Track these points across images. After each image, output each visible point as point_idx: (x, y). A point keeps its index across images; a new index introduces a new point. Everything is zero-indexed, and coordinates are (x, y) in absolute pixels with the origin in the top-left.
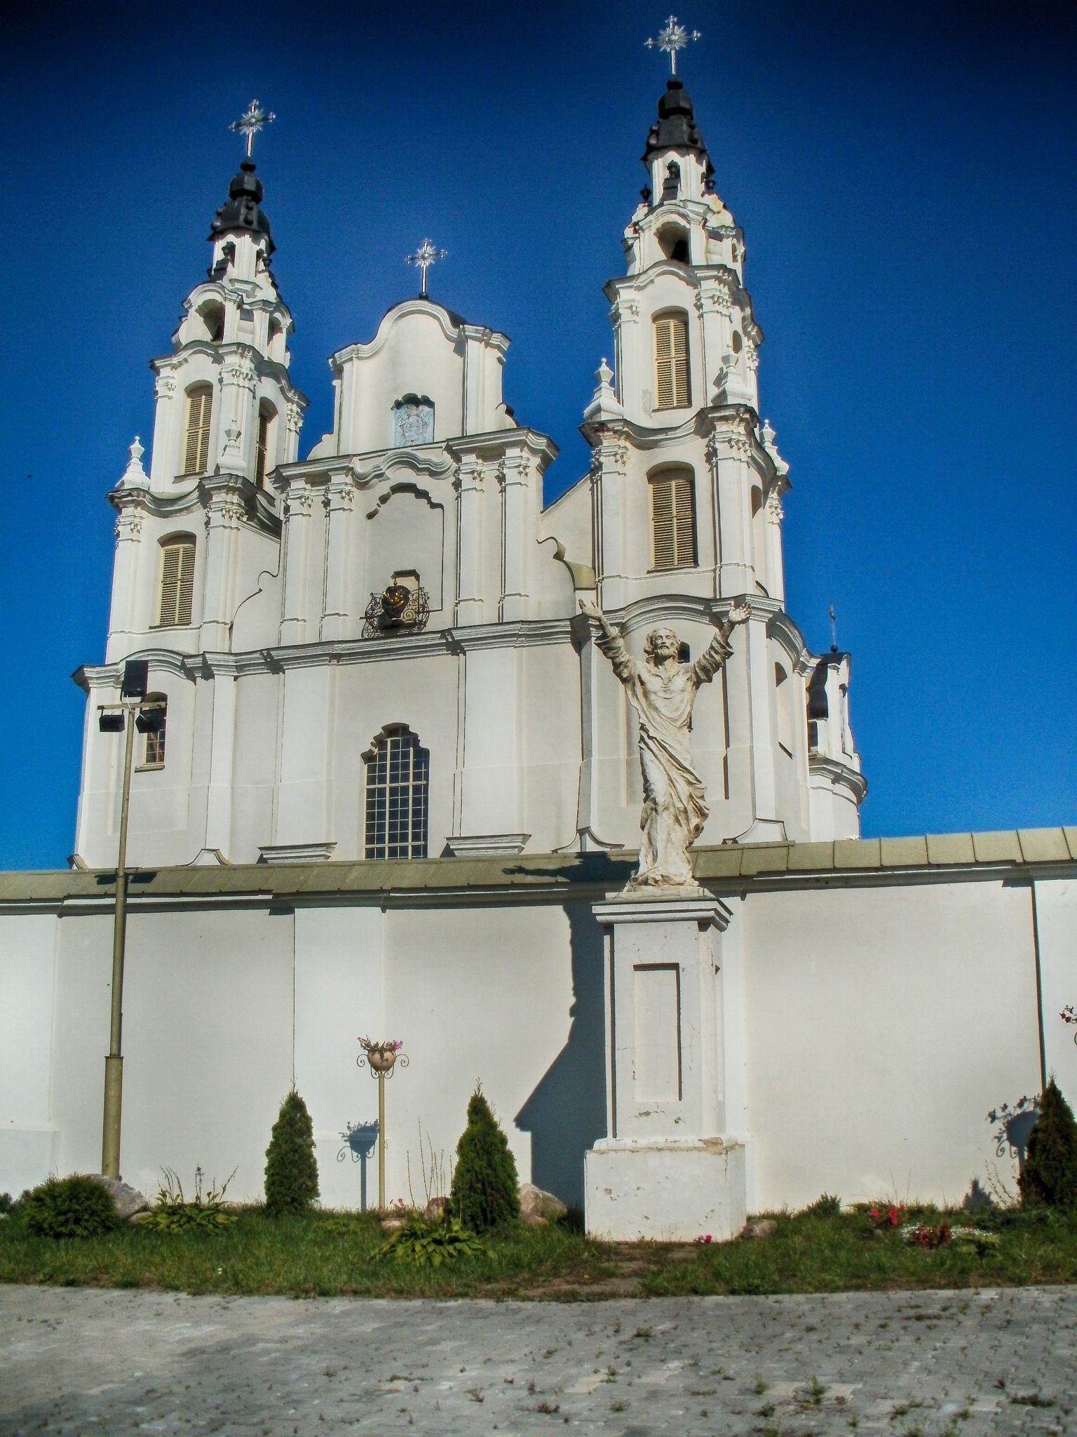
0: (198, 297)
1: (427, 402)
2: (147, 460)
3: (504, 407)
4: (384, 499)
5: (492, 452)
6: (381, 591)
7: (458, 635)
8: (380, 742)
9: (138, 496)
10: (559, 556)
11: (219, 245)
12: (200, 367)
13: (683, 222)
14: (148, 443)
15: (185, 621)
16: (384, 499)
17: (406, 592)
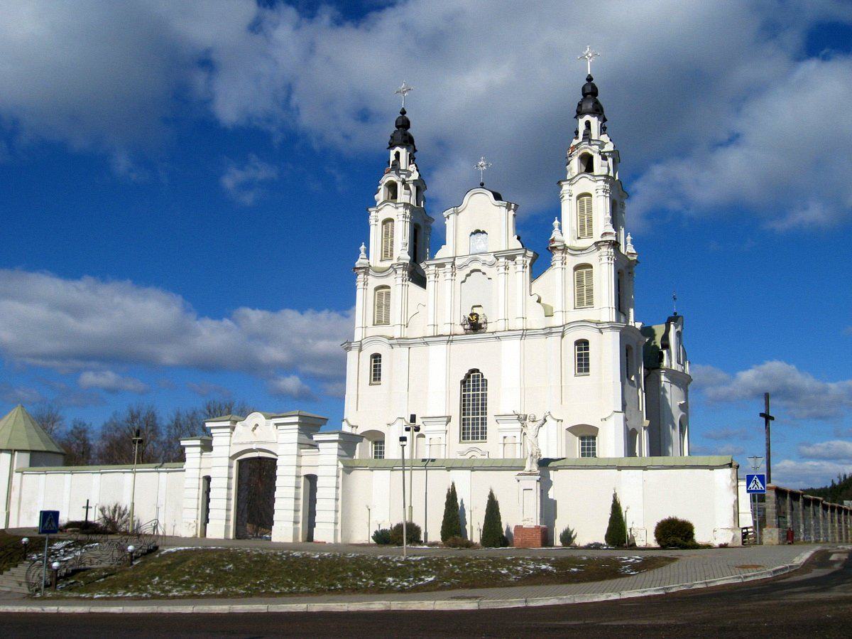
0: (387, 179)
1: (484, 232)
2: (367, 252)
3: (516, 236)
4: (468, 275)
5: (512, 258)
6: (468, 315)
7: (498, 334)
8: (468, 376)
9: (366, 270)
10: (539, 301)
11: (393, 153)
12: (388, 211)
13: (590, 152)
14: (368, 245)
15: (387, 323)
16: (468, 275)
17: (477, 315)
